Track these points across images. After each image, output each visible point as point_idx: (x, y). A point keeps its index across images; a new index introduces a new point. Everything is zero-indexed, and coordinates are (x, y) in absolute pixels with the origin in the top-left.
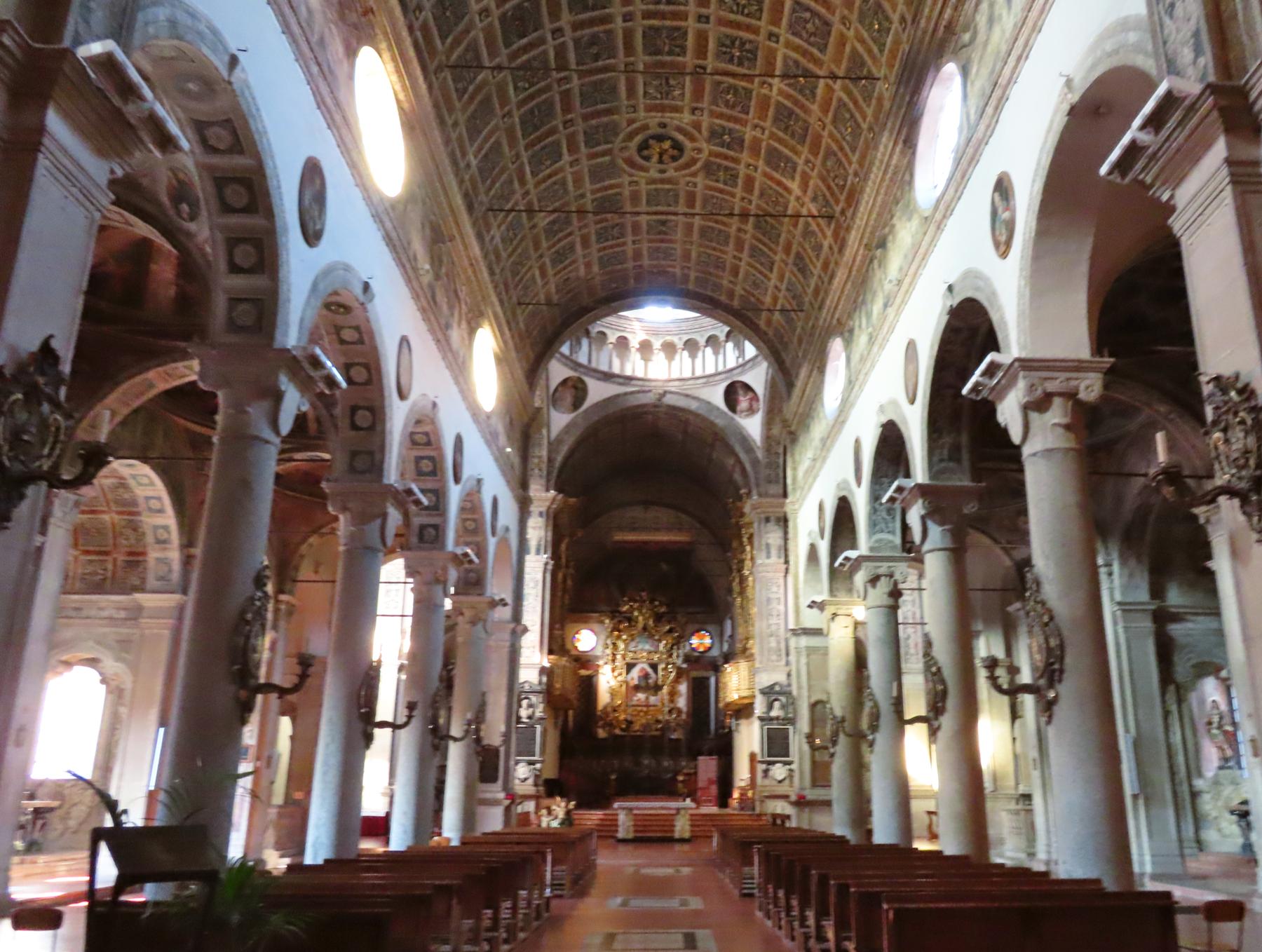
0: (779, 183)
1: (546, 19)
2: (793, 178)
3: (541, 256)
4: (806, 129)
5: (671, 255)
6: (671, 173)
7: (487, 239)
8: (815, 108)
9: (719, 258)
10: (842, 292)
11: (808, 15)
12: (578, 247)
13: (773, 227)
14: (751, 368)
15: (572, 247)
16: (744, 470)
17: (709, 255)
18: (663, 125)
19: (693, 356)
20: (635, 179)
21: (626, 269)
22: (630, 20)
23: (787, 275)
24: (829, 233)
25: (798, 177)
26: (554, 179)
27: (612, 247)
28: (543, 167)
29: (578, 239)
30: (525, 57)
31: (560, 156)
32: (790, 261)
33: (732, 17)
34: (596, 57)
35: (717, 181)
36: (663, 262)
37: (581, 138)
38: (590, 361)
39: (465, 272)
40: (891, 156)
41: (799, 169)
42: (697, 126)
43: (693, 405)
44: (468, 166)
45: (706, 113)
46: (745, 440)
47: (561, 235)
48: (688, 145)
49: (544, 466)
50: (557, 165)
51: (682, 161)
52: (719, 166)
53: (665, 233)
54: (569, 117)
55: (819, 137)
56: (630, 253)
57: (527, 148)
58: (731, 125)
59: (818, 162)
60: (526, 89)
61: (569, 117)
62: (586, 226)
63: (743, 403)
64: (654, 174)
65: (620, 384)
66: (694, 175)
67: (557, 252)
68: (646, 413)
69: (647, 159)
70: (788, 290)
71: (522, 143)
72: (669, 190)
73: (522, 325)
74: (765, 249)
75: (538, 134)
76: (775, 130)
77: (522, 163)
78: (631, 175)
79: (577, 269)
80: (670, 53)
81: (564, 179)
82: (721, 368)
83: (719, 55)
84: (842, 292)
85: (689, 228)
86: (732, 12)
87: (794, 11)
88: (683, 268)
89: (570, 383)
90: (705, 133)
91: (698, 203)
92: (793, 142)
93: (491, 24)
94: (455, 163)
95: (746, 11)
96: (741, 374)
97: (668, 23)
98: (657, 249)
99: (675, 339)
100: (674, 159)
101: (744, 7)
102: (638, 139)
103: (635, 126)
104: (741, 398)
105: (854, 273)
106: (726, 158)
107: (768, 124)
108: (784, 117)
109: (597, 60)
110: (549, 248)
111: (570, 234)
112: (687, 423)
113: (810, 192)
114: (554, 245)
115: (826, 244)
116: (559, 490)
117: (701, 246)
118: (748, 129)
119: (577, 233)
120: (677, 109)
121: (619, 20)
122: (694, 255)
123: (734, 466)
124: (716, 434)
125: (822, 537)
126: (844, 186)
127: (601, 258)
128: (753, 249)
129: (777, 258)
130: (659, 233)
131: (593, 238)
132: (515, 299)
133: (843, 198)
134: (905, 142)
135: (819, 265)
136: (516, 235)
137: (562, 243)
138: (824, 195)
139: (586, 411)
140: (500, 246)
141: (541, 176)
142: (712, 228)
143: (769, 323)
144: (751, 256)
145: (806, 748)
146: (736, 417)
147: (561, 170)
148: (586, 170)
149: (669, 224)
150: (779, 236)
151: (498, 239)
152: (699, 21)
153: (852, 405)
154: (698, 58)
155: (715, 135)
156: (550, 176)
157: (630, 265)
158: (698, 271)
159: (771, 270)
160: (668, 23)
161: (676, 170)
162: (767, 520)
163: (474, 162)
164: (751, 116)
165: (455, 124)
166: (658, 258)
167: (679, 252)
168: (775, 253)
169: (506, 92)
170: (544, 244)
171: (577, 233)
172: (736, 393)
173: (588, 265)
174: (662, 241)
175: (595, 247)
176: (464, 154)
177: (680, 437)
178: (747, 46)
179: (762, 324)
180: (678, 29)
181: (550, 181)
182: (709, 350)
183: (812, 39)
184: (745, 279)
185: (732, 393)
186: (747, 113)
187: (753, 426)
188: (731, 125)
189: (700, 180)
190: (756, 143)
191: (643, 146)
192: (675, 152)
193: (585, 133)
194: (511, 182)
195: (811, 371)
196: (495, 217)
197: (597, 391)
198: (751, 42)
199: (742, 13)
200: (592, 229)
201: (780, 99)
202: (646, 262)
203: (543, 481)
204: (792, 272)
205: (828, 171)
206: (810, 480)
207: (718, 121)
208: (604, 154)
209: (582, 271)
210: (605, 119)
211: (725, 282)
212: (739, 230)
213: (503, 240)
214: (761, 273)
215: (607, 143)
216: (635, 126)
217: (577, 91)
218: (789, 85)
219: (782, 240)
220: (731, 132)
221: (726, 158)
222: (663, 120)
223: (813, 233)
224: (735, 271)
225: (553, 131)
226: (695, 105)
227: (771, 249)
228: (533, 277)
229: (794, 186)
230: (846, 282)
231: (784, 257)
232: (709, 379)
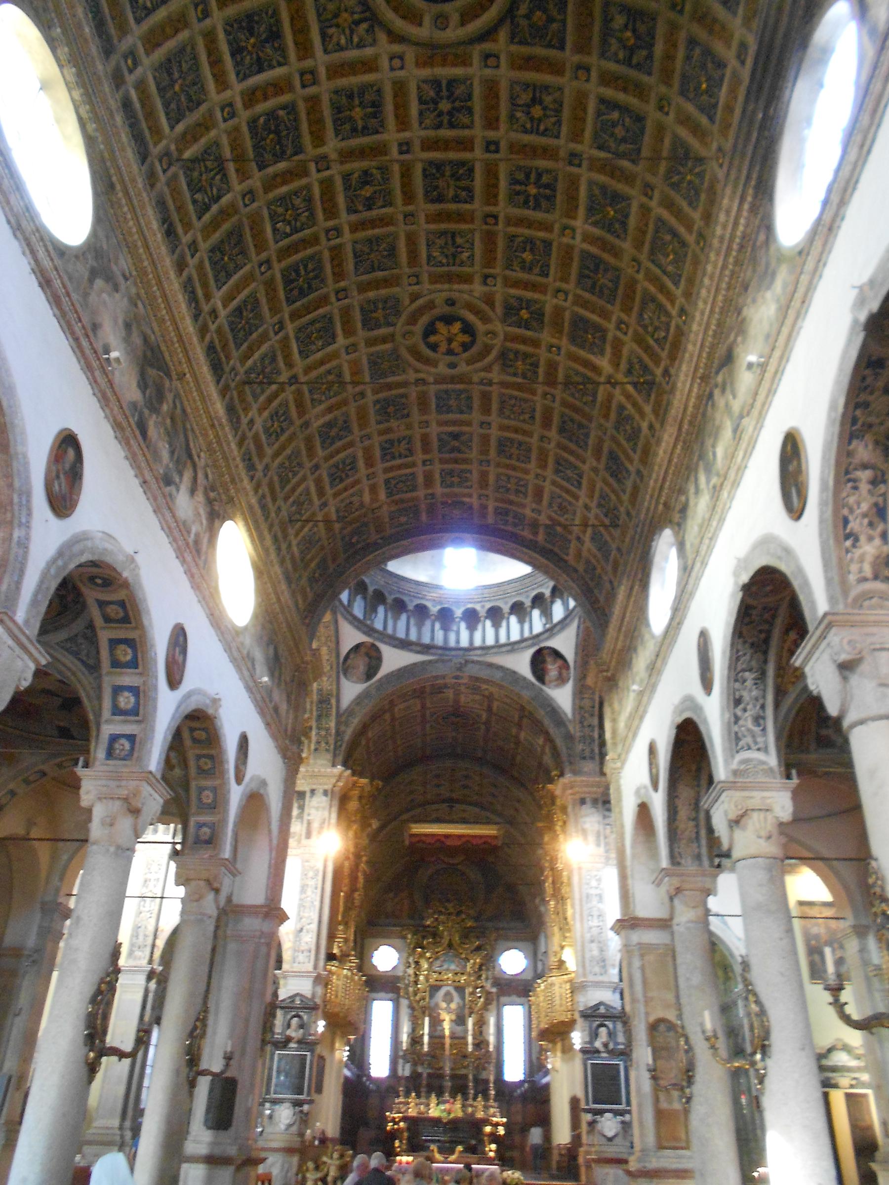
0: (587, 364)
1: (307, 139)
2: (602, 353)
3: (317, 467)
4: (616, 281)
5: (467, 480)
6: (463, 368)
7: (245, 421)
8: (627, 246)
9: (520, 479)
10: (670, 461)
11: (615, 115)
12: (361, 463)
13: (581, 426)
14: (563, 629)
15: (353, 466)
16: (554, 748)
17: (509, 477)
18: (451, 302)
19: (496, 625)
20: (421, 375)
21: (416, 499)
22: (407, 152)
23: (599, 485)
24: (648, 409)
25: (608, 350)
26: (328, 366)
27: (400, 467)
28: (314, 347)
29: (360, 454)
30: (284, 189)
31: (334, 337)
32: (602, 466)
33: (527, 138)
34: (369, 204)
35: (515, 375)
36: (456, 490)
37: (357, 315)
38: (385, 627)
39: (205, 435)
40: (736, 224)
41: (610, 336)
42: (489, 301)
43: (498, 675)
44: (214, 313)
45: (499, 280)
46: (554, 711)
47: (339, 444)
48: (480, 327)
49: (332, 740)
50: (329, 349)
51: (474, 350)
52: (517, 353)
53: (459, 451)
54: (342, 284)
55: (632, 285)
56: (421, 479)
57: (294, 316)
58: (529, 295)
59: (632, 320)
60: (288, 235)
61: (342, 284)
62: (369, 437)
63: (552, 669)
64: (442, 369)
65: (418, 652)
66: (488, 369)
67: (336, 466)
68: (446, 686)
69: (434, 347)
70: (599, 505)
71: (286, 311)
72: (461, 392)
73: (295, 549)
74: (572, 459)
75: (305, 300)
76: (579, 292)
77: (286, 338)
78: (417, 371)
79: (360, 493)
80: (456, 199)
81: (340, 367)
82: (527, 634)
83: (513, 196)
84: (670, 461)
85: (485, 439)
86: (526, 131)
87: (599, 114)
88: (480, 496)
89: (363, 650)
90: (499, 310)
91: (495, 406)
92: (601, 302)
93: (237, 129)
94: (193, 298)
95: (542, 128)
96: (547, 639)
97: (452, 155)
98: (451, 473)
99: (478, 607)
100: (466, 347)
101: (540, 120)
102: (424, 320)
103: (421, 302)
104: (550, 667)
105: (686, 426)
106: (524, 341)
107: (571, 286)
108: (593, 272)
109: (370, 208)
110: (326, 459)
111: (351, 444)
112: (490, 698)
113: (624, 366)
114: (332, 456)
115: (645, 425)
116: (345, 764)
117: (498, 465)
118: (548, 297)
119: (359, 445)
120: (467, 279)
121: (394, 151)
122: (492, 479)
123: (543, 746)
124: (523, 708)
125: (656, 789)
126: (665, 338)
127: (387, 482)
128: (559, 462)
129: (586, 468)
130: (452, 450)
131: (378, 453)
132: (284, 513)
133: (664, 354)
134: (757, 188)
135: (636, 457)
136: (283, 430)
137: (342, 455)
138: (641, 361)
139: (380, 680)
140: (263, 438)
141: (311, 359)
142: (512, 441)
143: (579, 555)
144: (557, 471)
145: (646, 1085)
146: (544, 688)
147: (335, 355)
148: (365, 361)
149: (463, 438)
150: (587, 435)
151: (258, 426)
152: (487, 150)
153: (692, 595)
154: (488, 204)
155: (511, 311)
156: (322, 363)
157: (421, 493)
158: (496, 500)
159: (579, 485)
160: (452, 155)
161: (469, 362)
162: (583, 802)
163: (223, 313)
164: (551, 278)
165: (194, 247)
166: (451, 485)
167: (475, 476)
168: (584, 462)
169: (262, 231)
170: (320, 453)
171: (359, 445)
172: (544, 662)
173: (373, 489)
174: (456, 461)
175: (380, 466)
176: (208, 297)
177: (484, 716)
178: (545, 179)
179: (570, 558)
180: (463, 163)
181: (322, 369)
182: (513, 619)
183: (623, 148)
184: (550, 505)
185: (542, 659)
186: (547, 275)
187: (563, 697)
188: (529, 295)
189: (495, 375)
190: (558, 311)
191: (430, 330)
192: (466, 338)
193: (362, 309)
194: (274, 359)
195: (632, 588)
196: (256, 397)
197: (393, 660)
198: (548, 171)
199: (537, 133)
200: (377, 440)
201: (585, 246)
202: (439, 490)
203: (329, 756)
204: (605, 481)
205: (645, 327)
206: (636, 723)
207: (513, 291)
208: (384, 340)
209: (367, 498)
210: (383, 292)
211: (528, 512)
212: (542, 438)
213: (266, 430)
214: (568, 492)
215: (390, 324)
216: (421, 302)
217: (349, 249)
218: (595, 224)
219: (591, 441)
220: (529, 303)
221: (524, 341)
222: (455, 295)
223: (629, 418)
224: (539, 494)
225: (324, 300)
226: (486, 271)
227: (578, 457)
228: (307, 492)
229: (604, 363)
230: (675, 446)
231: (595, 464)
232: (513, 647)
